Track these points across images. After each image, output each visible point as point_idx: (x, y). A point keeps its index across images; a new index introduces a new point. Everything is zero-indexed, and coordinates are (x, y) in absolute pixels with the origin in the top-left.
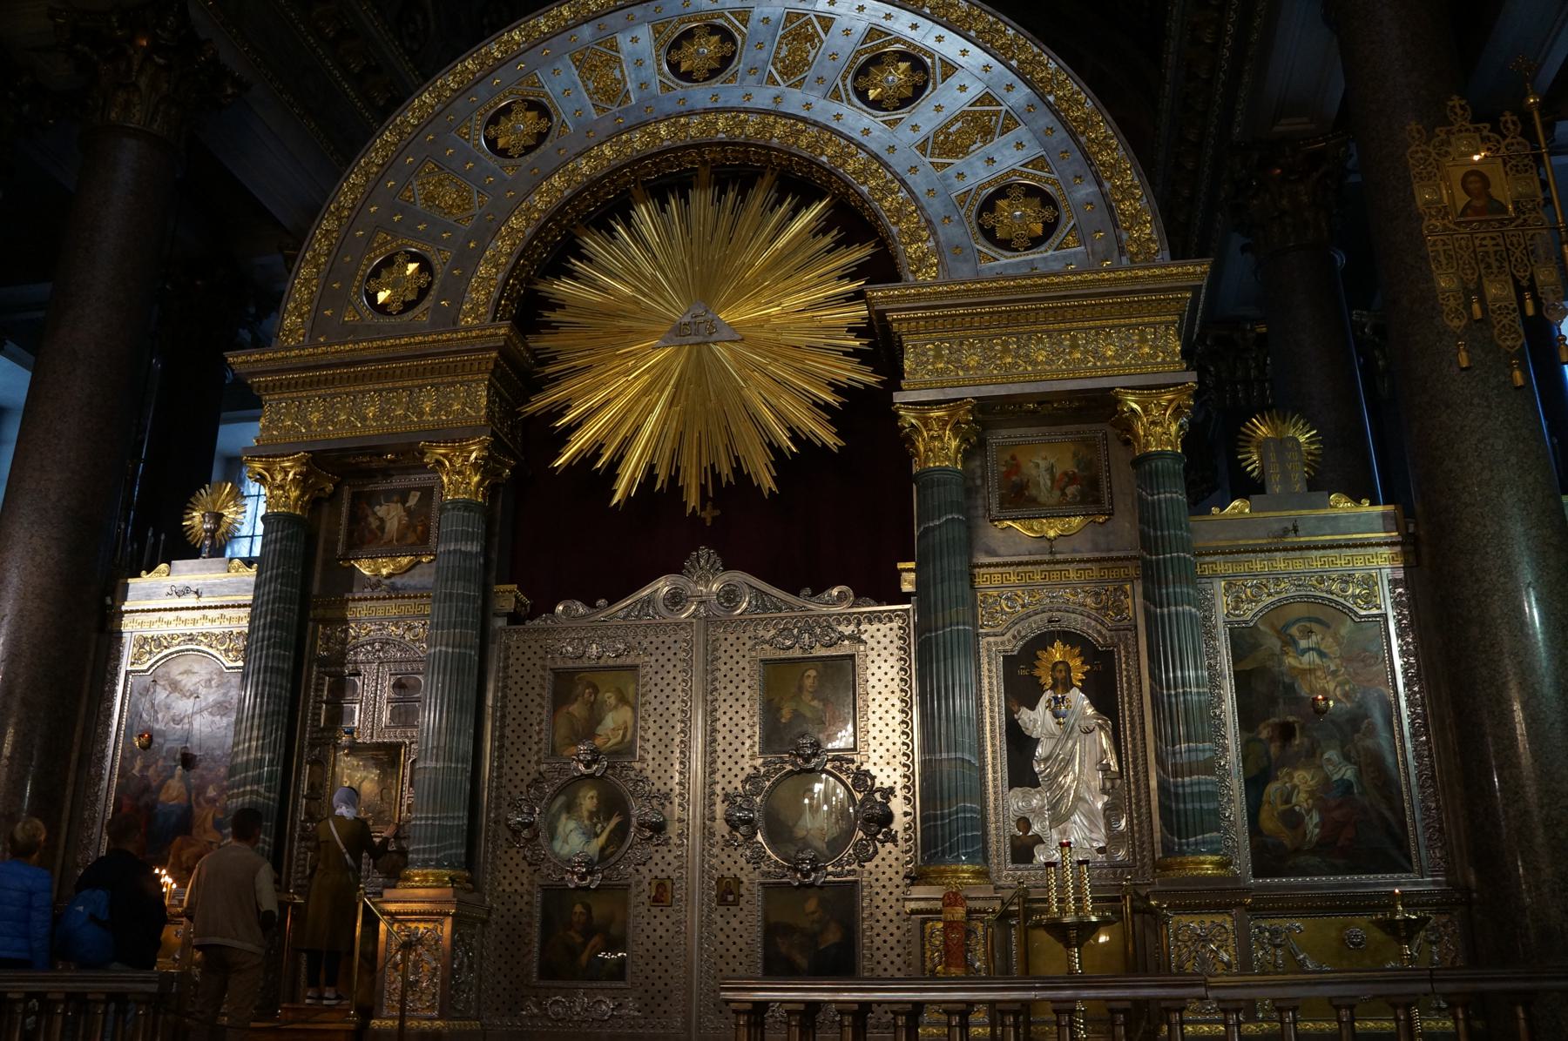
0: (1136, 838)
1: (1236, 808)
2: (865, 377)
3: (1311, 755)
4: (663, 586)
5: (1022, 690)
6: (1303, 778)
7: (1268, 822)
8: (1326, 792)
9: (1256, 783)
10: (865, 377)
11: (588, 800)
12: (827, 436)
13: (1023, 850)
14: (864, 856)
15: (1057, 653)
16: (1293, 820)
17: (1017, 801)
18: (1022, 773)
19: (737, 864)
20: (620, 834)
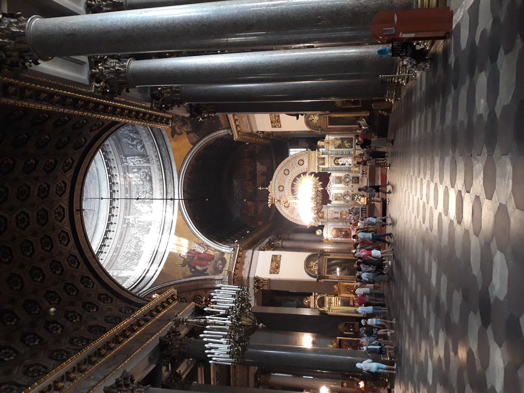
0: (350, 157)
1: (348, 149)
2: (313, 175)
3: (344, 144)
4: (328, 191)
5: (338, 164)
6: (346, 144)
7: (349, 147)
8: (347, 142)
9: (346, 148)
10: (313, 175)
11: (345, 197)
12: (318, 178)
13: (350, 165)
14: (350, 176)
15: (336, 162)
16: (349, 145)
17: (347, 165)
18: (345, 164)
19: (350, 186)
20: (348, 195)
